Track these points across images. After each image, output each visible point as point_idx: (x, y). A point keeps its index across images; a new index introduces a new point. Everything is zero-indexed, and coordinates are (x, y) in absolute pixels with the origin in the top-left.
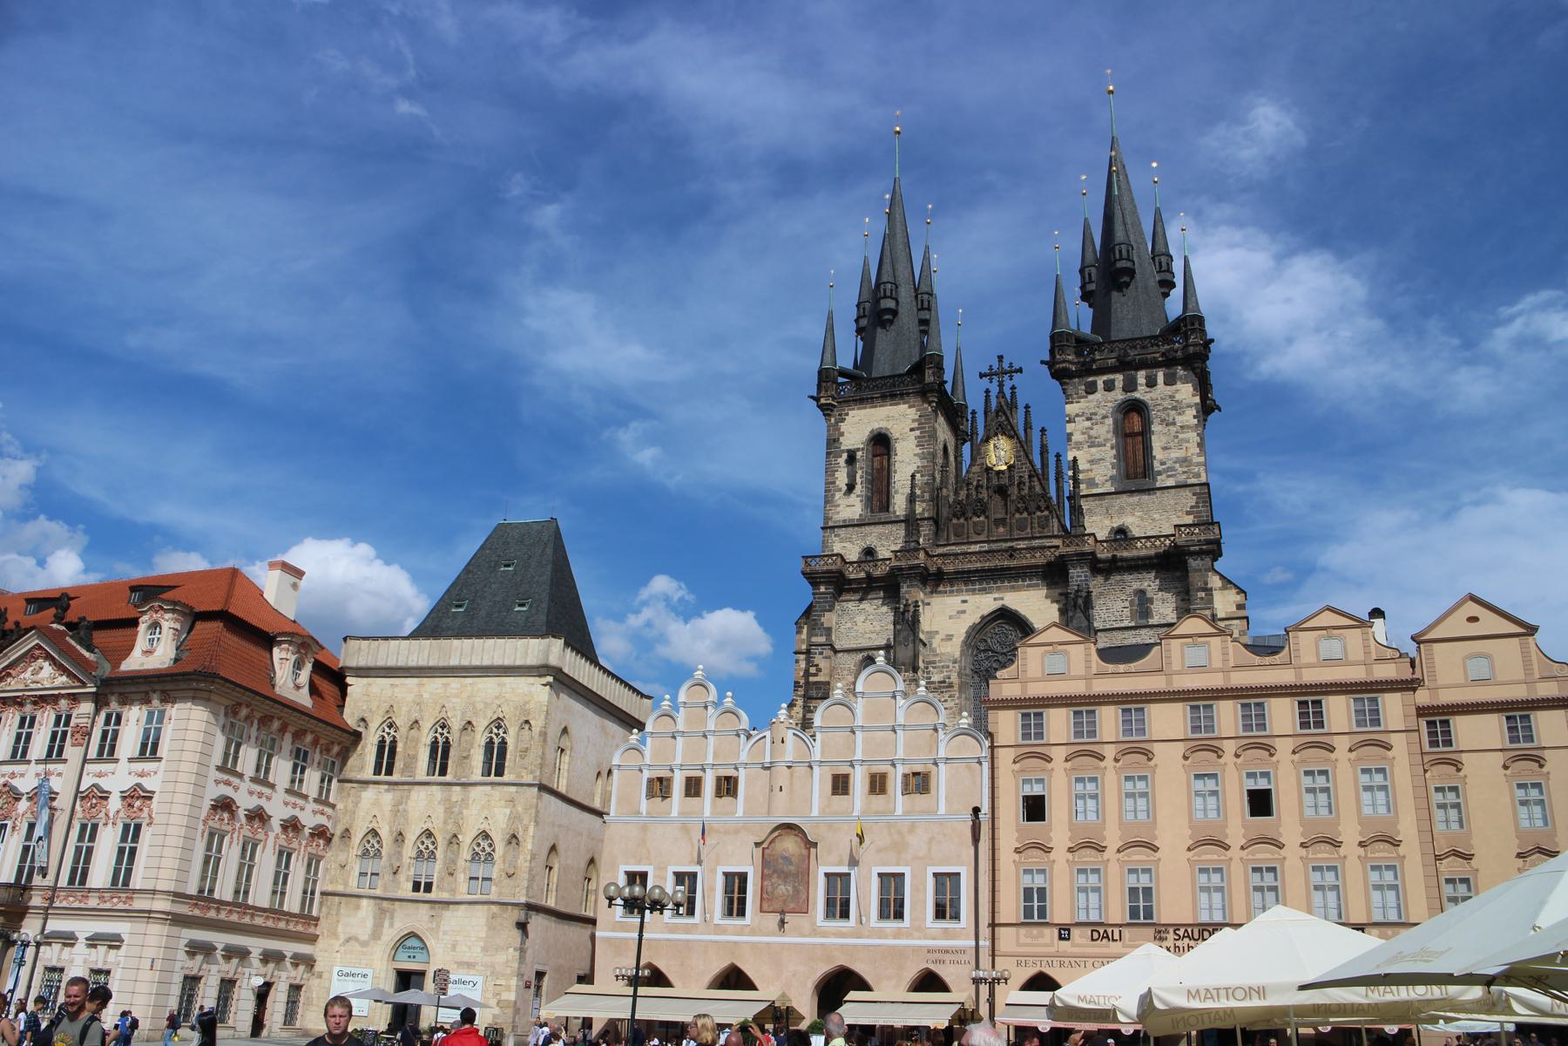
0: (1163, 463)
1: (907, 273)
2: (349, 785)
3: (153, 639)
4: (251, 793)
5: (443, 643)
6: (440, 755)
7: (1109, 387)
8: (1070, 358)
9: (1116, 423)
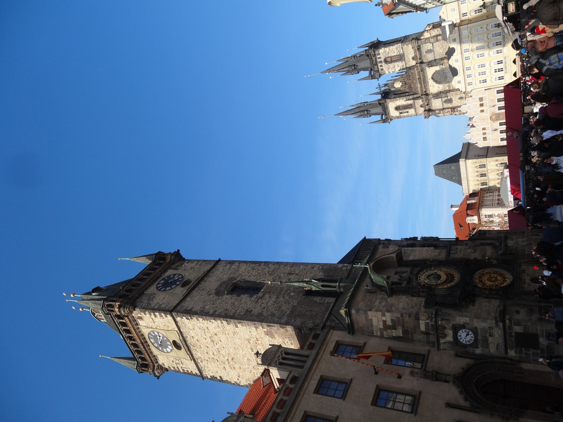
0: (398, 53)
1: (357, 109)
2: (490, 189)
4: (495, 201)
5: (462, 178)
6: (483, 175)
7: (381, 66)
8: (376, 75)
9: (389, 63)
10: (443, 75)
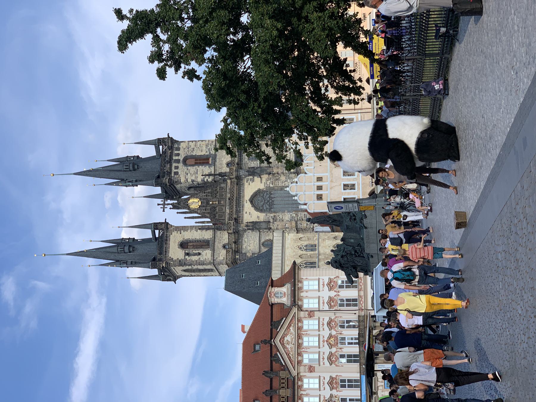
0: (207, 152)
3: (280, 296)
7: (177, 168)
10: (268, 201)
